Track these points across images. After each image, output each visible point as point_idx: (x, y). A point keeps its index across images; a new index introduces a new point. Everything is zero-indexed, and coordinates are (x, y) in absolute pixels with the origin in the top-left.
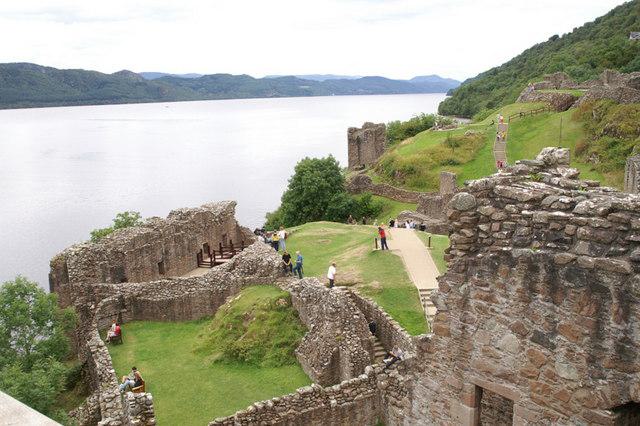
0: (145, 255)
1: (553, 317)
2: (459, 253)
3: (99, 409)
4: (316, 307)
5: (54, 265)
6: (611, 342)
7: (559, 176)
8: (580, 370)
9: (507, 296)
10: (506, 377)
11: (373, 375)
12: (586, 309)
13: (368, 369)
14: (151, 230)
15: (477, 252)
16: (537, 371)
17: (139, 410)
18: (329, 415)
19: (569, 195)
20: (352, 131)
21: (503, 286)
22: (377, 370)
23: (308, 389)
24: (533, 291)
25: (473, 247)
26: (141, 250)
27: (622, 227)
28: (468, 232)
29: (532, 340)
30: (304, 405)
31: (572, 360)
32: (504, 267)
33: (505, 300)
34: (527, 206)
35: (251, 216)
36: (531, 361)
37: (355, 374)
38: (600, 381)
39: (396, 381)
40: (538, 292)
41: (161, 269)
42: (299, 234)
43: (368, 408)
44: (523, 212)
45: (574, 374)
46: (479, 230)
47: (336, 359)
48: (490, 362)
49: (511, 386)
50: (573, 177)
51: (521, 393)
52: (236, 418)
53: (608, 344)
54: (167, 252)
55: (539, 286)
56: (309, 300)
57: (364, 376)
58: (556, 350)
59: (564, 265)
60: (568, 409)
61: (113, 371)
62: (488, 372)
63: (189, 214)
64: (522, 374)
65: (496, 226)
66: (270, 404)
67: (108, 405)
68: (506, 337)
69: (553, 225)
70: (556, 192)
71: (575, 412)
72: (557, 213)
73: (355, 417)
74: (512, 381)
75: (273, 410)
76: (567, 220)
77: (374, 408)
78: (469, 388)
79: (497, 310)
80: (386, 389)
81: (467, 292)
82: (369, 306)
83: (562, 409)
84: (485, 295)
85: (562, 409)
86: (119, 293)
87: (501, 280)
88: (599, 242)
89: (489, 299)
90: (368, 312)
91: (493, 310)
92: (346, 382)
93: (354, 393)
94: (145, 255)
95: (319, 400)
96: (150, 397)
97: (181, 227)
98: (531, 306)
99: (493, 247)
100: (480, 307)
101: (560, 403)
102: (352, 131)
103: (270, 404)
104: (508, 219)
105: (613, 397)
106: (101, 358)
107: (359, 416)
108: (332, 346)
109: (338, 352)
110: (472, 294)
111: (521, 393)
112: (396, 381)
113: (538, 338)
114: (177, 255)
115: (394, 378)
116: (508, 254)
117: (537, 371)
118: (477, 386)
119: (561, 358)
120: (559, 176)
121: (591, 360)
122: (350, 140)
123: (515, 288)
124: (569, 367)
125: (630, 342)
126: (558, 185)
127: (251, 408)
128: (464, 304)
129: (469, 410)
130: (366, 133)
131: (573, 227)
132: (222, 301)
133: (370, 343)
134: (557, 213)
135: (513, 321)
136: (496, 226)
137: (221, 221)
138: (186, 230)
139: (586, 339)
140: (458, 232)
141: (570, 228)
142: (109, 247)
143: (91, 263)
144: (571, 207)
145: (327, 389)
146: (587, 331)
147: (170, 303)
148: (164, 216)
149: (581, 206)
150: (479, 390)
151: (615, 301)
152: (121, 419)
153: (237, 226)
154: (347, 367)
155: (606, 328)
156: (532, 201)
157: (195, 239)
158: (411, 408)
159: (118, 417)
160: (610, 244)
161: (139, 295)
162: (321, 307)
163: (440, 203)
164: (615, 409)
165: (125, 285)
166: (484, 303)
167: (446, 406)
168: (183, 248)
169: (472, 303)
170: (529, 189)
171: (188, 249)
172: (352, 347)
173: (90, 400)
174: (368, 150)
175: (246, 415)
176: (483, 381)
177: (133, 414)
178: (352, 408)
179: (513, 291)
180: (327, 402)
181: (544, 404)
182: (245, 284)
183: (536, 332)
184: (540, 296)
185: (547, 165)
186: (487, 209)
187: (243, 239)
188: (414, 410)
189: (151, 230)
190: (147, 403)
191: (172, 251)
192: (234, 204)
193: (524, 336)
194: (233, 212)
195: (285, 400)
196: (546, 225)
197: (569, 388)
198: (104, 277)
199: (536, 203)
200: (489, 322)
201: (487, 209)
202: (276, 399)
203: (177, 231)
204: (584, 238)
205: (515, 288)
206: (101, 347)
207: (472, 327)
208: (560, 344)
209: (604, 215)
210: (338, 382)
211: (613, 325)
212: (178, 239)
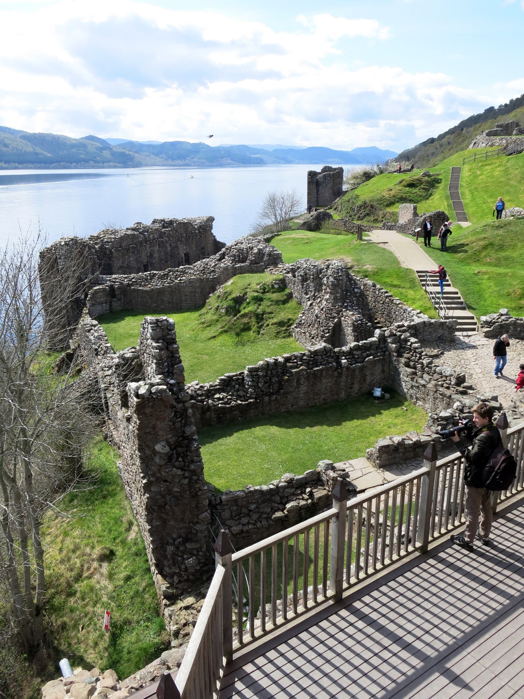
0: (131, 254)
11: (383, 338)
13: (377, 332)
17: (160, 335)
18: (340, 374)
20: (312, 175)
39: (409, 343)
43: (378, 369)
52: (246, 372)
54: (151, 256)
56: (304, 279)
63: (171, 222)
66: (281, 359)
73: (365, 380)
77: (383, 371)
82: (365, 285)
86: (108, 283)
92: (353, 344)
93: (364, 354)
94: (131, 254)
95: (330, 360)
97: (165, 233)
102: (312, 175)
107: (369, 379)
108: (334, 318)
112: (409, 343)
114: (161, 260)
127: (261, 363)
130: (325, 175)
132: (213, 289)
137: (199, 232)
142: (96, 244)
145: (337, 350)
147: (160, 292)
148: (148, 222)
153: (215, 240)
157: (177, 247)
159: (133, 350)
161: (129, 285)
168: (167, 254)
171: (171, 256)
175: (256, 370)
178: (362, 369)
180: (339, 363)
182: (235, 272)
191: (156, 255)
192: (211, 219)
194: (211, 227)
195: (296, 357)
202: (285, 355)
212: (161, 245)
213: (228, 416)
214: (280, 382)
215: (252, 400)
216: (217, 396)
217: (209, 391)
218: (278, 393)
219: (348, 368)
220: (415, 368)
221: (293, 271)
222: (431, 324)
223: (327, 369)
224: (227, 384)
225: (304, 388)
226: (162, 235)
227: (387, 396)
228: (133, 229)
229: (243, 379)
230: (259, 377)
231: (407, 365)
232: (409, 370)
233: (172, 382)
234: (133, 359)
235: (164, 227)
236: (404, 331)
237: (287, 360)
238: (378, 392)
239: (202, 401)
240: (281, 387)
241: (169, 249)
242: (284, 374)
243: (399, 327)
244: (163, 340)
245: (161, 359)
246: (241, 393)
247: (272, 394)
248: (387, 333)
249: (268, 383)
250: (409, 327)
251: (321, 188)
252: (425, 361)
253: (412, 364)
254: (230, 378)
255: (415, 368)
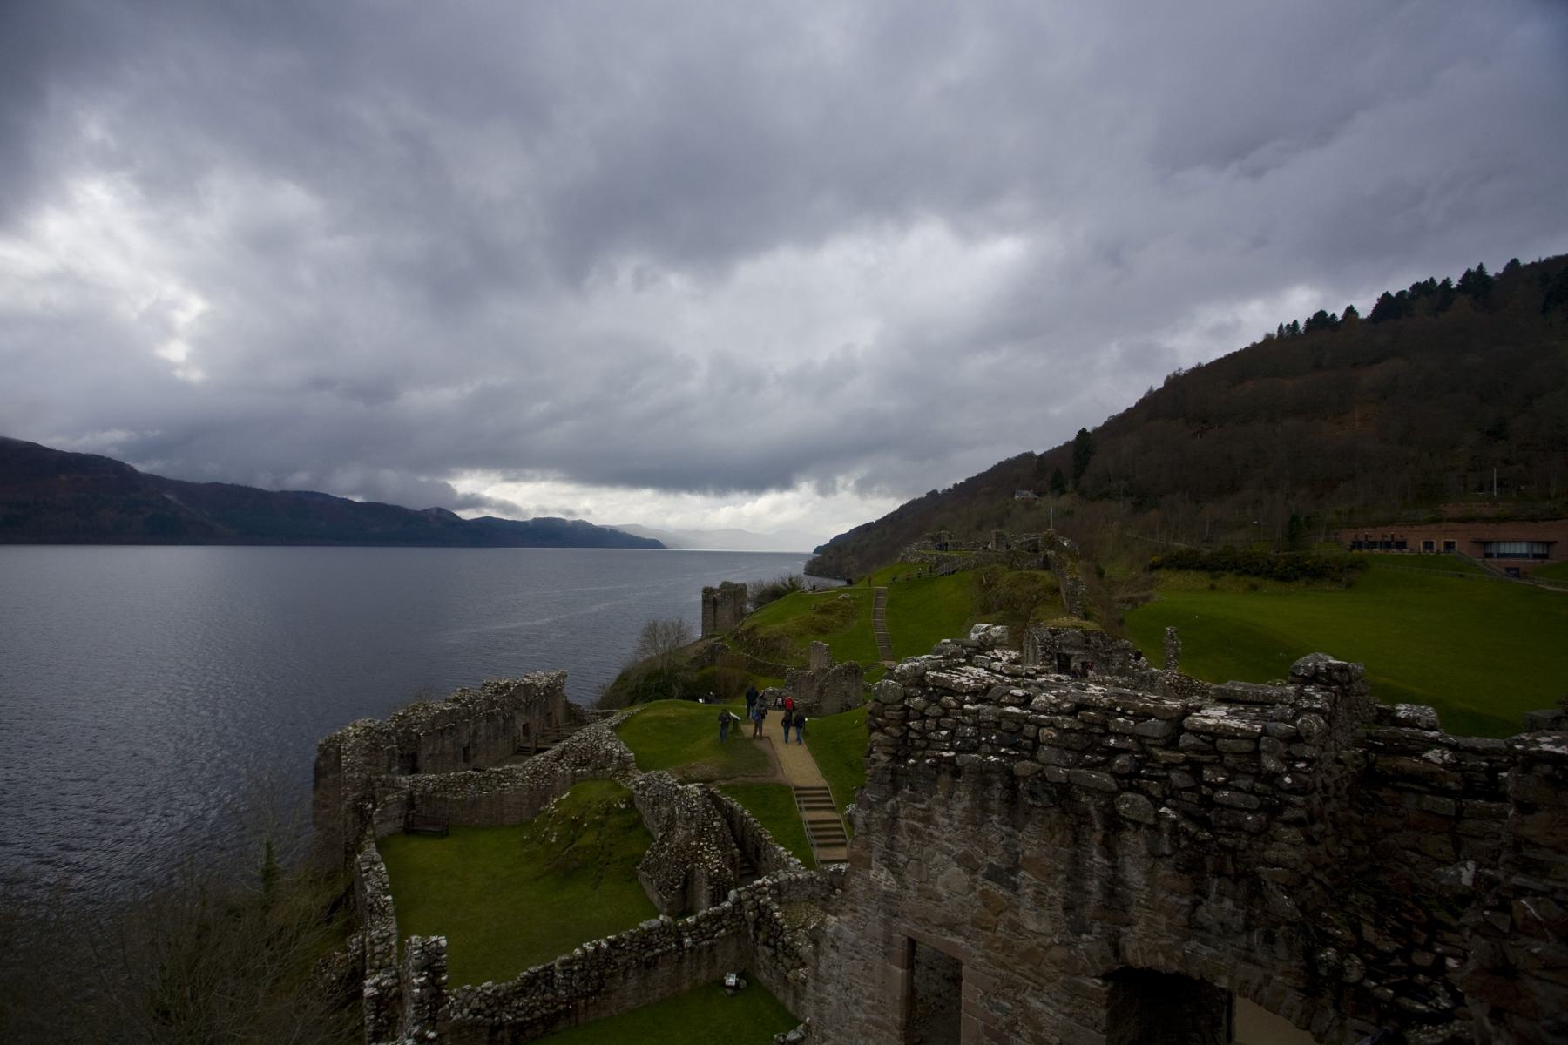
1: (1015, 846)
2: (884, 758)
3: (364, 954)
4: (665, 810)
5: (324, 751)
6: (1096, 882)
7: (999, 660)
8: (1054, 920)
9: (950, 817)
10: (952, 927)
11: (739, 903)
12: (1058, 836)
13: (732, 893)
14: (457, 706)
15: (907, 757)
16: (995, 919)
19: (1025, 687)
20: (708, 592)
21: (943, 803)
22: (744, 896)
23: (655, 922)
24: (986, 811)
25: (902, 748)
26: (441, 732)
27: (1098, 730)
28: (896, 732)
29: (987, 876)
30: (650, 946)
31: (1042, 906)
32: (945, 778)
33: (947, 821)
34: (968, 698)
35: (581, 695)
36: (986, 905)
37: (714, 902)
38: (1084, 936)
40: (993, 812)
41: (466, 755)
42: (649, 715)
44: (967, 706)
45: (1045, 926)
46: (909, 728)
47: (688, 880)
48: (930, 904)
49: (959, 940)
50: (1015, 662)
51: (974, 952)
53: (1093, 885)
54: (475, 734)
55: (994, 805)
57: (727, 904)
58: (1020, 892)
59: (1025, 778)
60: (1040, 974)
61: (389, 898)
62: (925, 920)
63: (507, 686)
64: (974, 923)
65: (930, 723)
66: (604, 945)
67: (378, 949)
68: (948, 872)
69: (1005, 724)
70: (1001, 681)
71: (1050, 980)
72: (1010, 709)
74: (959, 934)
75: (607, 953)
76: (1026, 719)
77: (739, 948)
78: (899, 940)
79: (936, 833)
80: (756, 922)
81: (895, 809)
83: (1032, 976)
84: (920, 813)
85: (1032, 976)
87: (941, 795)
88: (1069, 749)
89: (927, 819)
90: (730, 816)
91: (931, 835)
92: (702, 913)
96: (443, 943)
98: (984, 829)
99: (928, 752)
100: (913, 830)
101: (1028, 966)
102: (708, 592)
103: (604, 945)
104: (946, 715)
105: (1103, 959)
106: (373, 881)
107: (720, 960)
109: (693, 869)
110: (902, 813)
111: (974, 952)
113: (994, 874)
114: (489, 738)
115: (766, 906)
116: (951, 760)
117: (995, 919)
118: (910, 939)
119: (1027, 902)
120: (999, 660)
121: (1068, 908)
122: (704, 601)
123: (960, 806)
124: (1039, 916)
125: (1122, 882)
126: (1000, 672)
127: (578, 951)
128: (891, 824)
129: (899, 971)
131: (1033, 728)
133: (733, 858)
134: (1010, 709)
135: (959, 850)
136: (930, 723)
138: (502, 706)
139: (1061, 877)
140: (883, 731)
141: (1030, 730)
143: (375, 747)
144: (1025, 702)
146: (1061, 867)
149: (1041, 699)
150: (912, 943)
151: (1098, 827)
152: (397, 976)
154: (703, 893)
155: (1088, 863)
156: (974, 692)
157: (512, 718)
158: (817, 968)
160: (1084, 751)
161: (434, 791)
162: (673, 810)
163: (812, 678)
164: (1105, 977)
165: (418, 777)
166: (920, 825)
167: (866, 966)
169: (903, 823)
170: (971, 675)
172: (713, 860)
173: (353, 942)
174: (726, 614)
175: (571, 962)
176: (918, 930)
177: (416, 970)
178: (711, 947)
179: (958, 810)
180: (680, 943)
181: (1003, 966)
183: (991, 865)
184: (995, 818)
185: (984, 646)
186: (918, 701)
187: (576, 717)
188: (822, 970)
189: (457, 706)
190: (439, 951)
193: (974, 871)
196: (998, 725)
197: (1040, 945)
198: (390, 767)
199: (981, 694)
200: (926, 851)
201: (918, 701)
203: (491, 707)
204: (1052, 744)
205: (960, 806)
206: (375, 863)
207: (902, 857)
208: (1024, 883)
209: (1072, 713)
210: (691, 912)
211: (1098, 858)
213: (528, 1033)
214: (600, 977)
215: (561, 1007)
216: (516, 1003)
217: (505, 996)
218: (597, 992)
219: (691, 949)
220: (775, 947)
221: (644, 788)
222: (797, 880)
223: (662, 954)
224: (531, 981)
225: (633, 983)
226: (492, 704)
227: (743, 983)
228: (456, 700)
229: (553, 975)
230: (573, 972)
231: (766, 943)
232: (768, 951)
233: (432, 1035)
234: (390, 988)
235: (496, 692)
236: (765, 893)
237: (612, 944)
238: (731, 980)
239: (493, 1016)
240: (601, 986)
241: (501, 721)
242: (607, 964)
243: (759, 886)
244: (430, 970)
245: (422, 1001)
246: (549, 996)
247: (590, 994)
248: (744, 896)
249: (586, 979)
250: (771, 887)
251: (719, 609)
252: (787, 939)
253: (771, 942)
254: (536, 975)
255: (775, 947)
